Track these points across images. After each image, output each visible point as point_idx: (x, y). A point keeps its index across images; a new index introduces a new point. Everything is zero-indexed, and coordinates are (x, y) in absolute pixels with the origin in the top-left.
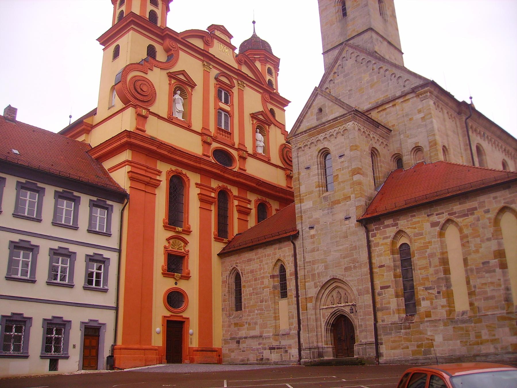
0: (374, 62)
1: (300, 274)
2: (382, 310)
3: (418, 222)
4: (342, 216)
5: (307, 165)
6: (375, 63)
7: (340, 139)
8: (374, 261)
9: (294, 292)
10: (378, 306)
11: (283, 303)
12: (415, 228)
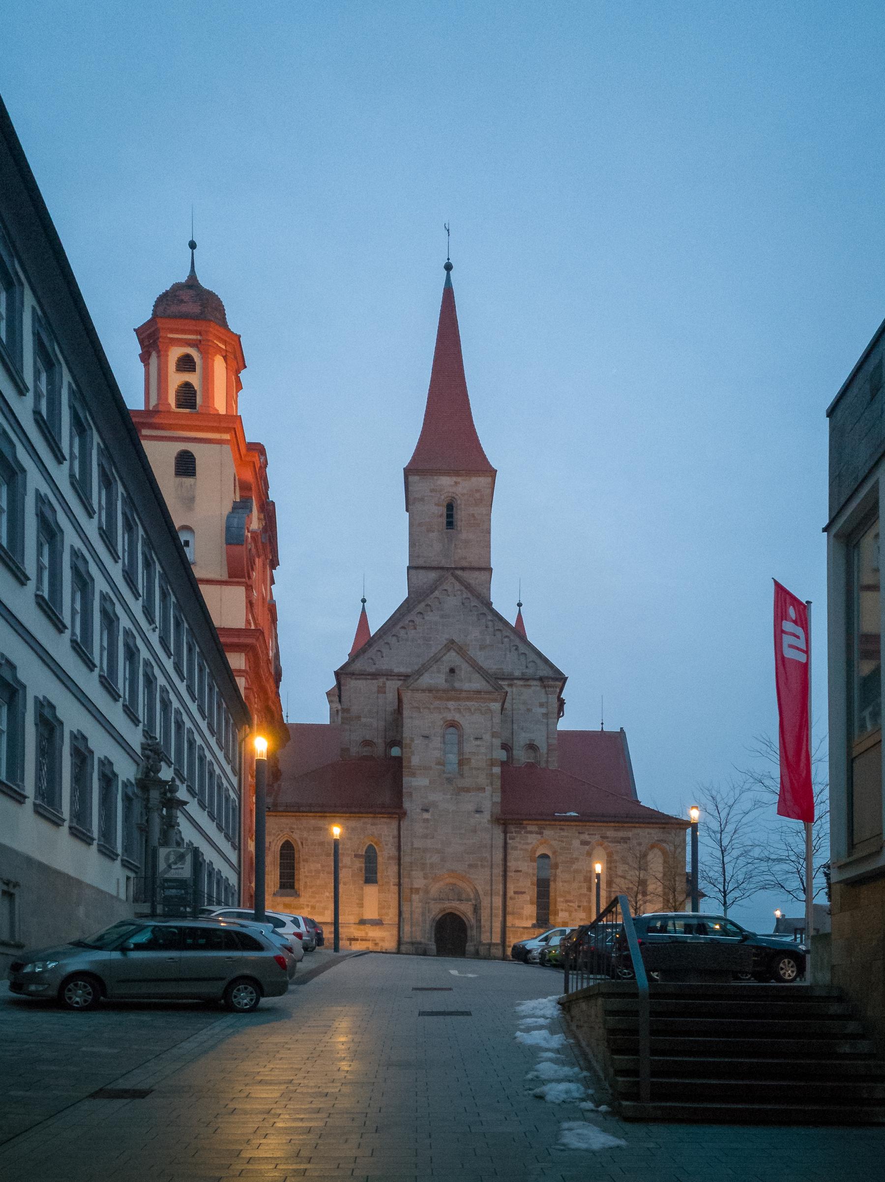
0: (489, 618)
1: (406, 859)
2: (513, 914)
3: (567, 837)
4: (471, 807)
6: (491, 621)
8: (508, 864)
10: (509, 909)
11: (371, 891)
12: (562, 841)
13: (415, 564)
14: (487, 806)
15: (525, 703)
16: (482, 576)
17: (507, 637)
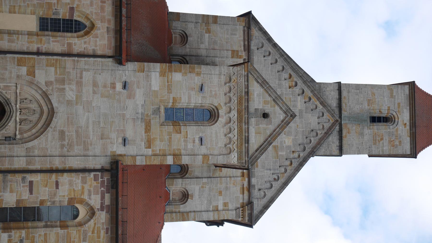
0: (302, 155)
1: (69, 61)
3: (99, 237)
4: (129, 134)
5: (205, 88)
6: (299, 156)
7: (222, 141)
8: (65, 174)
9: (44, 48)
10: (9, 177)
11: (31, 23)
12: (93, 232)
13: (342, 86)
14: (131, 150)
15: (227, 188)
16: (335, 148)
17: (286, 171)
